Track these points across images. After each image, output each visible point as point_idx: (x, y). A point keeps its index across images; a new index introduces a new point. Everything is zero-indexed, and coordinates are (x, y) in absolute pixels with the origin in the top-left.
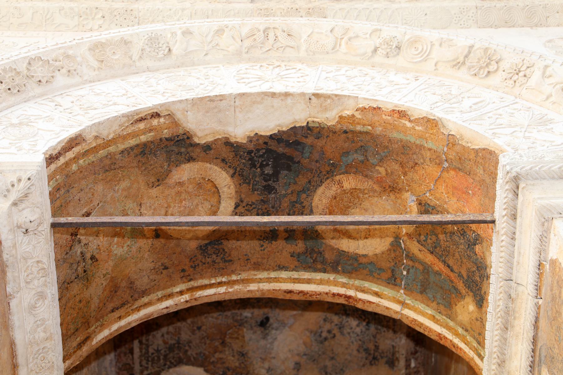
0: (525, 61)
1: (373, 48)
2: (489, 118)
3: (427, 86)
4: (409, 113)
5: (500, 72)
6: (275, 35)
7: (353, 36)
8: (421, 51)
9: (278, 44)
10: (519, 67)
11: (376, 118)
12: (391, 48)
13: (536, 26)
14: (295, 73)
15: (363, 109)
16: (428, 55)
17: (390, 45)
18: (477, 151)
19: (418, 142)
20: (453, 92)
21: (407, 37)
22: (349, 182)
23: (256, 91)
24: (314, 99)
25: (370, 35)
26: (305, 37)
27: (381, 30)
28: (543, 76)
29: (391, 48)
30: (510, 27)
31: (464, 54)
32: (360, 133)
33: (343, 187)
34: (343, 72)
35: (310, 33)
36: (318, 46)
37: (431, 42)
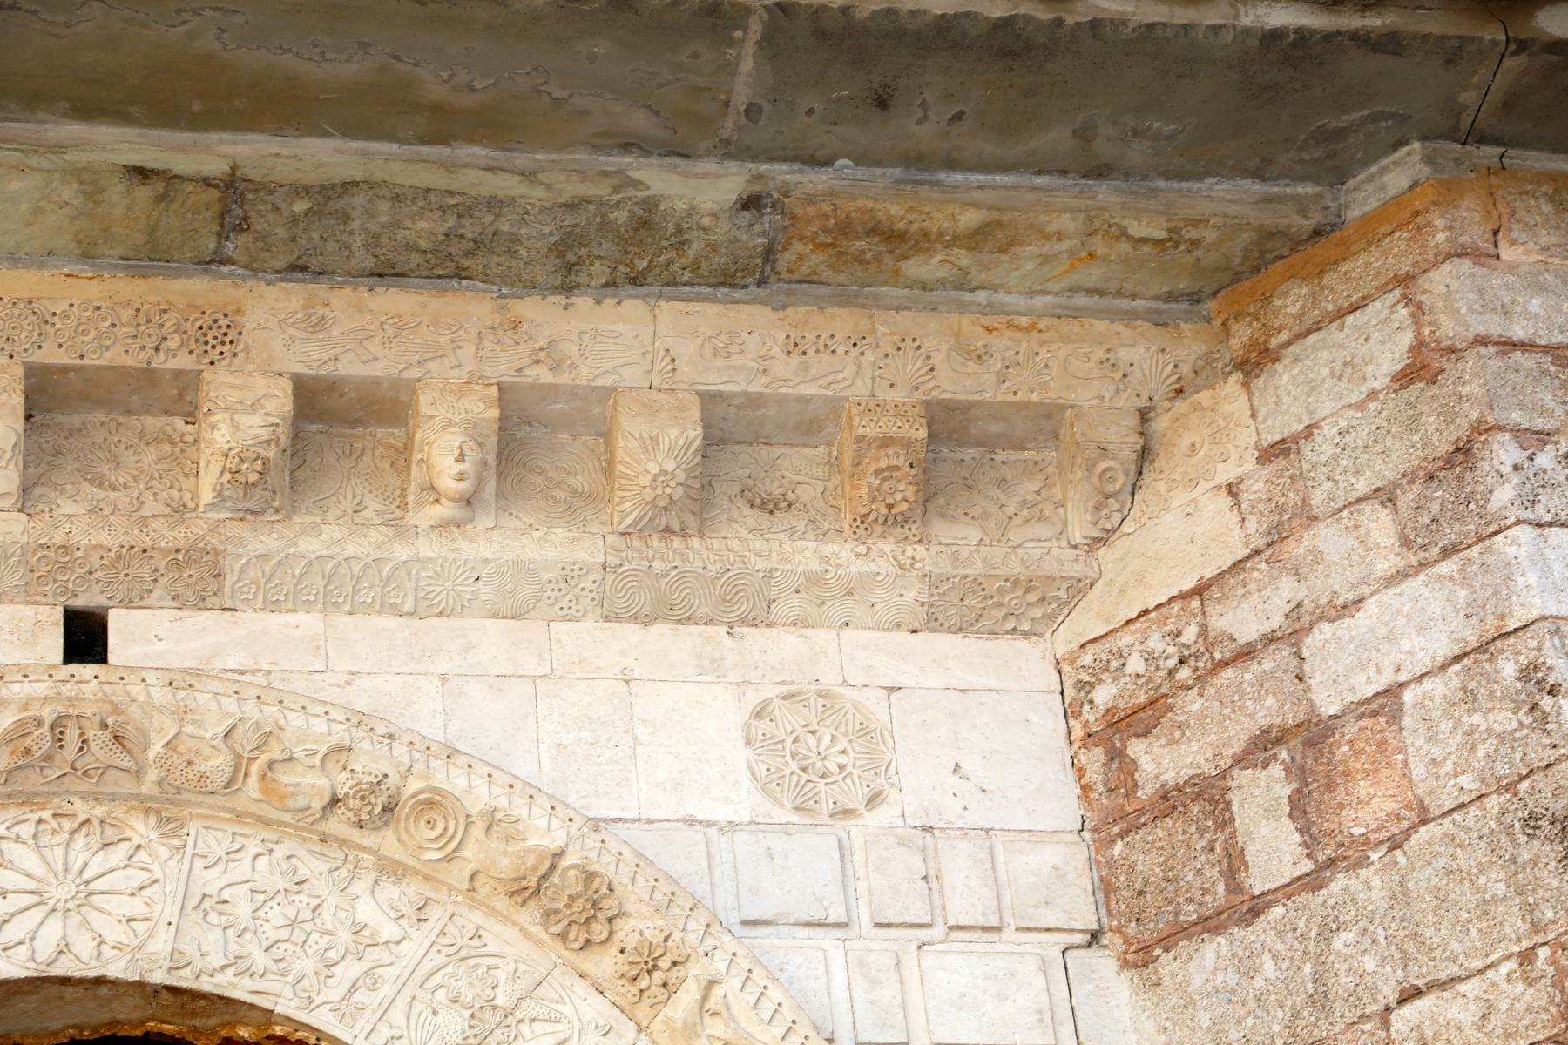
0: (670, 943)
1: (327, 799)
3: (442, 959)
5: (613, 950)
6: (82, 734)
8: (442, 835)
9: (86, 761)
12: (369, 813)
13: (743, 621)
14: (126, 866)
20: (499, 1002)
21: (414, 785)
23: (22, 974)
24: (165, 995)
25: (323, 760)
26: (157, 748)
29: (369, 813)
30: (679, 622)
34: (242, 869)
36: (190, 776)
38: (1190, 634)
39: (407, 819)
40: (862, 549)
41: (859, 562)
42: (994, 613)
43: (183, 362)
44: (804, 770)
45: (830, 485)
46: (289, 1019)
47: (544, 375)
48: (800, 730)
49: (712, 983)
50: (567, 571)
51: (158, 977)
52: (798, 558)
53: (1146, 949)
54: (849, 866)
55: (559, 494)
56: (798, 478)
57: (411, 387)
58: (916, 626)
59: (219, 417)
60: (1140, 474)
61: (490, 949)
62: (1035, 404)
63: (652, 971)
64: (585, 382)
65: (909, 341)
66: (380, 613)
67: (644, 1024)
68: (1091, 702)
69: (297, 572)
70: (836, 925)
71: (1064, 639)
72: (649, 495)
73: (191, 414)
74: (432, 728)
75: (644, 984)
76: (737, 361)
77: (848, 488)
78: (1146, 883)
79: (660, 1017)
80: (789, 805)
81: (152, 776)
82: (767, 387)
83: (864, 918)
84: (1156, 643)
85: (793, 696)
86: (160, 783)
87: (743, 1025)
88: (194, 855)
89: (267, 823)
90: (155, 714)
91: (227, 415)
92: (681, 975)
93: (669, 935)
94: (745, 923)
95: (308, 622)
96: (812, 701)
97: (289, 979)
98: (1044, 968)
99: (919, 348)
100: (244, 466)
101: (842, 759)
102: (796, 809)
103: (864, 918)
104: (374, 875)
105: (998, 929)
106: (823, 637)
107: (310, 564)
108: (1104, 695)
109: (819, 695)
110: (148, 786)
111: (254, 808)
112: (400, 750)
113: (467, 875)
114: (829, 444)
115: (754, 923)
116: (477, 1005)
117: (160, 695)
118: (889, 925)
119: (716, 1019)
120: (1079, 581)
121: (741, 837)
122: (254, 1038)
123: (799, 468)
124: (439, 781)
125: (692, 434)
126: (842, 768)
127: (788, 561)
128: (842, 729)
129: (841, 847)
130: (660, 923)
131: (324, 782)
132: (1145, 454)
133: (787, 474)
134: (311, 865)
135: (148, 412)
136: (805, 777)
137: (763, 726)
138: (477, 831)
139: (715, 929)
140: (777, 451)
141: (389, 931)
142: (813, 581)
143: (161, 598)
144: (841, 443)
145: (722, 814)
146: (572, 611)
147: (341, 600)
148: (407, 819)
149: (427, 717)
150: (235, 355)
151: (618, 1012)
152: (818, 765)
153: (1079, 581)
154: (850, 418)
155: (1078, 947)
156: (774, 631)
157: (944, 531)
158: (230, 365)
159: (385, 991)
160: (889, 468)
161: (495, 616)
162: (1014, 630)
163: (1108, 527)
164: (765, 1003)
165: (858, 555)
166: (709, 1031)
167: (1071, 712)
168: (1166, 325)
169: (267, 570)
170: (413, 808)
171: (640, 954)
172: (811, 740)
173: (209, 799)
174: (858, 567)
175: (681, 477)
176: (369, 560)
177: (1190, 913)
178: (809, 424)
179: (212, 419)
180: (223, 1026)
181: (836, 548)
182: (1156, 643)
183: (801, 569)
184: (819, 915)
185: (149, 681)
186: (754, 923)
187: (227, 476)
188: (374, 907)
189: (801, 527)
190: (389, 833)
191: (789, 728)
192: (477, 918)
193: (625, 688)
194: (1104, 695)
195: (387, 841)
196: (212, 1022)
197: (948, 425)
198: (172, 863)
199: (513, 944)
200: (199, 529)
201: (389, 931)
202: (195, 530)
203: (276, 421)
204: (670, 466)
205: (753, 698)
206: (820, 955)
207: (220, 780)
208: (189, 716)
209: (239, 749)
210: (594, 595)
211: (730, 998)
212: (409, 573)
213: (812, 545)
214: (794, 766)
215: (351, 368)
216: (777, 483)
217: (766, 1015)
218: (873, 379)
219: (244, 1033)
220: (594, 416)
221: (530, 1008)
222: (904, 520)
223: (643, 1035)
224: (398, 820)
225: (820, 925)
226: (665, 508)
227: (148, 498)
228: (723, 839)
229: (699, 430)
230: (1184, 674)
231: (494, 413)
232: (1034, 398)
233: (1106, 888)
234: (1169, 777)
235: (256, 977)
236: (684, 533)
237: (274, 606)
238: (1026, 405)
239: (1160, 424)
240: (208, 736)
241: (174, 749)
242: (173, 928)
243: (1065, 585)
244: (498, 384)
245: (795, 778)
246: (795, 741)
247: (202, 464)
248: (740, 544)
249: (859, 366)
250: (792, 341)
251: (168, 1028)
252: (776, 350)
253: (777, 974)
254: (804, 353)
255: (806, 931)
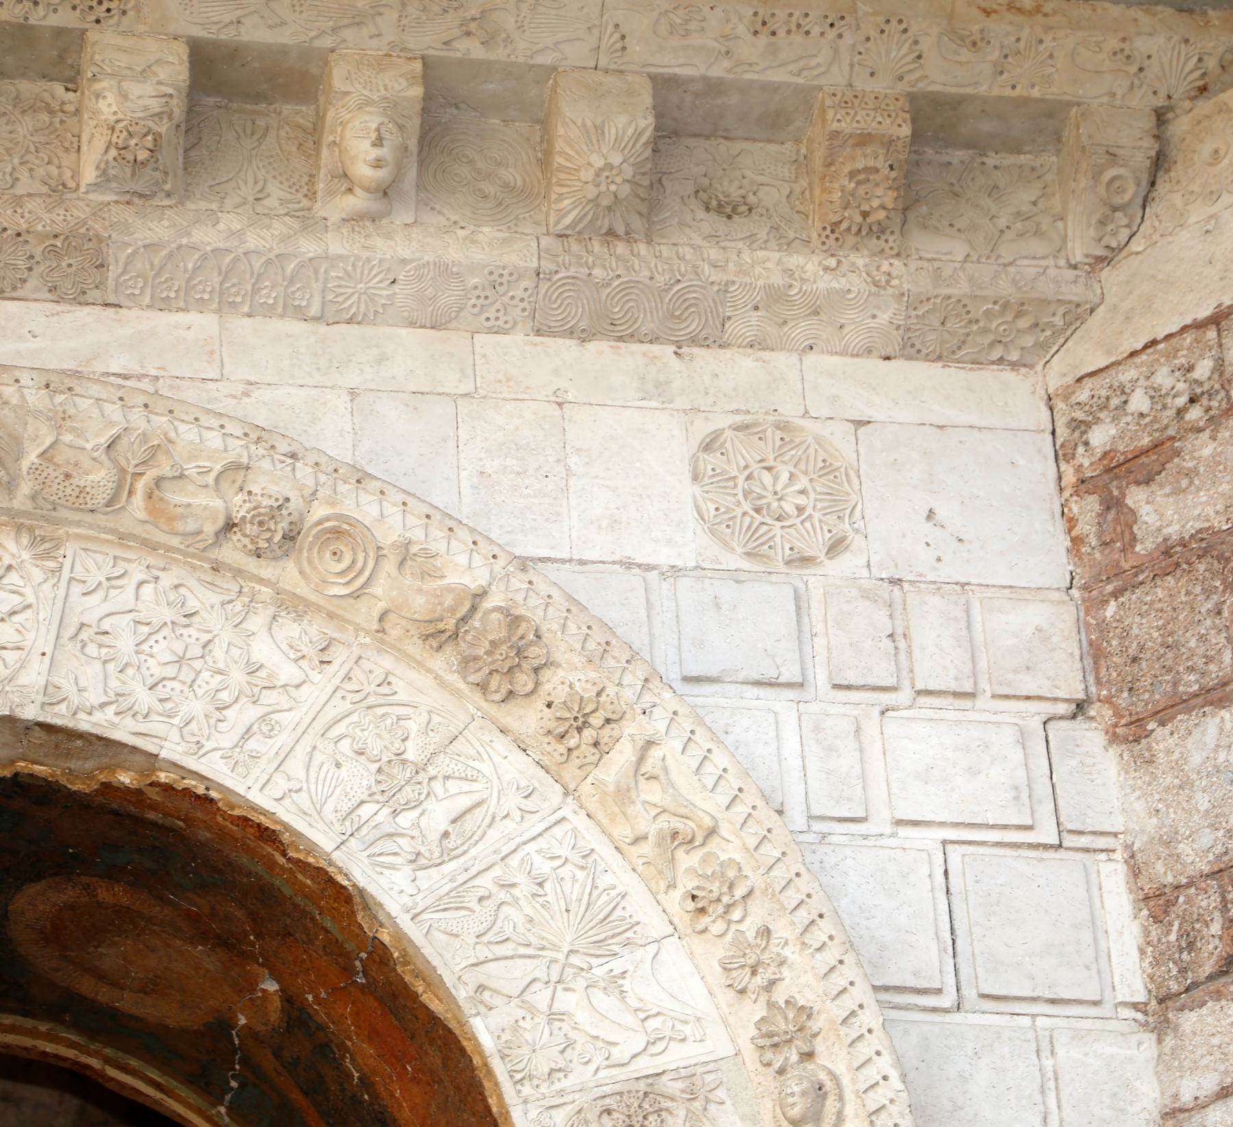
0: (603, 698)
1: (221, 523)
2: (481, 899)
3: (347, 706)
4: (286, 838)
7: (170, 475)
10: (587, 710)
11: (199, 814)
12: (268, 540)
13: (694, 341)
15: (168, 788)
16: (364, 586)
17: (269, 530)
18: (434, 1020)
19: (299, 900)
20: (409, 756)
21: (320, 511)
22: (112, 894)
25: (217, 479)
26: (31, 457)
27: (248, 468)
28: (636, 771)
29: (268, 540)
30: (620, 339)
31: (459, 615)
32: (154, 824)
33: (95, 896)
34: (125, 597)
35: (48, 441)
36: (68, 491)
37: (379, 548)
38: (1204, 369)
39: (310, 549)
40: (832, 262)
41: (827, 277)
42: (979, 339)
43: (64, 18)
44: (758, 510)
45: (797, 189)
46: (175, 765)
47: (474, 49)
48: (754, 467)
49: (650, 743)
50: (496, 277)
51: (30, 713)
52: (758, 270)
53: (1139, 722)
54: (806, 620)
55: (489, 188)
56: (760, 179)
57: (324, 58)
58: (890, 352)
59: (105, 84)
60: (1153, 184)
61: (401, 697)
62: (1037, 100)
63: (581, 728)
64: (521, 60)
65: (894, 23)
66: (282, 316)
67: (572, 786)
68: (1086, 444)
69: (190, 266)
70: (789, 685)
71: (1058, 373)
72: (591, 192)
73: (72, 80)
74: (341, 450)
75: (572, 742)
76: (696, 40)
77: (817, 191)
78: (1142, 649)
79: (589, 780)
80: (740, 550)
81: (25, 489)
82: (729, 71)
83: (820, 677)
84: (1163, 378)
85: (747, 427)
86: (33, 498)
87: (683, 792)
88: (71, 579)
89: (151, 546)
90: (30, 420)
91: (114, 82)
92: (615, 733)
93: (603, 689)
94: (687, 679)
95: (201, 324)
96: (769, 432)
97: (176, 721)
98: (1023, 740)
99: (905, 31)
100: (133, 142)
101: (801, 500)
102: (748, 554)
103: (820, 677)
104: (271, 610)
105: (971, 695)
106: (783, 361)
107: (204, 257)
108: (1100, 437)
109: (778, 428)
110: (21, 500)
111: (138, 530)
112: (304, 471)
113: (376, 614)
114: (797, 141)
115: (698, 680)
116: (385, 759)
117: (36, 398)
118: (849, 687)
119: (654, 785)
120: (1078, 305)
121: (685, 583)
122: (135, 785)
123: (761, 167)
124: (348, 507)
125: (643, 123)
126: (800, 510)
127: (746, 274)
128: (802, 466)
129: (797, 598)
130: (593, 675)
131: (218, 503)
132: (1160, 163)
133: (748, 173)
134: (200, 597)
135: (23, 76)
136: (759, 519)
137: (712, 460)
138: (389, 566)
139: (655, 684)
140: (738, 146)
141: (288, 672)
142: (775, 297)
143: (36, 290)
144: (811, 140)
145: (664, 557)
146: (500, 323)
147: (239, 299)
148: (310, 549)
149: (334, 435)
150: (124, 13)
151: (542, 773)
152: (773, 504)
153: (1078, 305)
154: (823, 111)
155: (1062, 718)
156: (728, 353)
157: (928, 245)
158: (118, 24)
159: (283, 739)
160: (867, 170)
161: (412, 324)
162: (1001, 360)
163: (1114, 244)
164: (708, 767)
165: (826, 269)
166: (643, 797)
167: (1062, 454)
168: (1190, 11)
169: (157, 261)
170: (317, 537)
171: (569, 709)
172: (767, 477)
173: (89, 518)
174: (825, 283)
175: (628, 172)
176: (272, 255)
177: (1191, 684)
178: (775, 117)
179: (97, 86)
180: (101, 769)
181: (802, 261)
182: (1163, 378)
183: (761, 282)
184: (771, 673)
185: (23, 382)
186: (698, 680)
187: (113, 153)
188: (273, 645)
189: (763, 235)
190: (290, 565)
191: (742, 464)
192: (387, 662)
193: (558, 412)
194: (1100, 437)
195: (288, 573)
196: (89, 765)
197: (936, 123)
198: (47, 587)
199: (426, 693)
200: (80, 212)
201: (288, 672)
202: (76, 213)
203: (170, 91)
204: (616, 159)
205: (702, 429)
206: (771, 718)
207: (101, 497)
208: (68, 423)
209: (123, 463)
210: (525, 304)
211: (669, 761)
212: (316, 272)
213: (776, 255)
214: (746, 506)
215: (256, 33)
216: (736, 183)
217: (710, 783)
218: (852, 66)
219: (125, 778)
220: (529, 100)
221: (444, 764)
222: (880, 230)
223: (570, 799)
224: (301, 551)
225: (771, 684)
226: (609, 208)
227: (24, 175)
228: (665, 585)
229: (651, 120)
230: (1195, 413)
231: (417, 91)
232: (1036, 93)
233: (1096, 654)
234: (1173, 531)
235: (139, 717)
236: (629, 237)
237: (163, 304)
238: (1026, 101)
239: (1180, 126)
240: (89, 446)
241: (50, 460)
242: (47, 659)
243: (1061, 310)
244: (423, 58)
245: (747, 520)
246: (749, 478)
247: (85, 138)
248: (693, 252)
249: (836, 50)
250: (760, 19)
251: (38, 769)
252: (741, 29)
253: (722, 736)
254: (773, 33)
255: (755, 691)
